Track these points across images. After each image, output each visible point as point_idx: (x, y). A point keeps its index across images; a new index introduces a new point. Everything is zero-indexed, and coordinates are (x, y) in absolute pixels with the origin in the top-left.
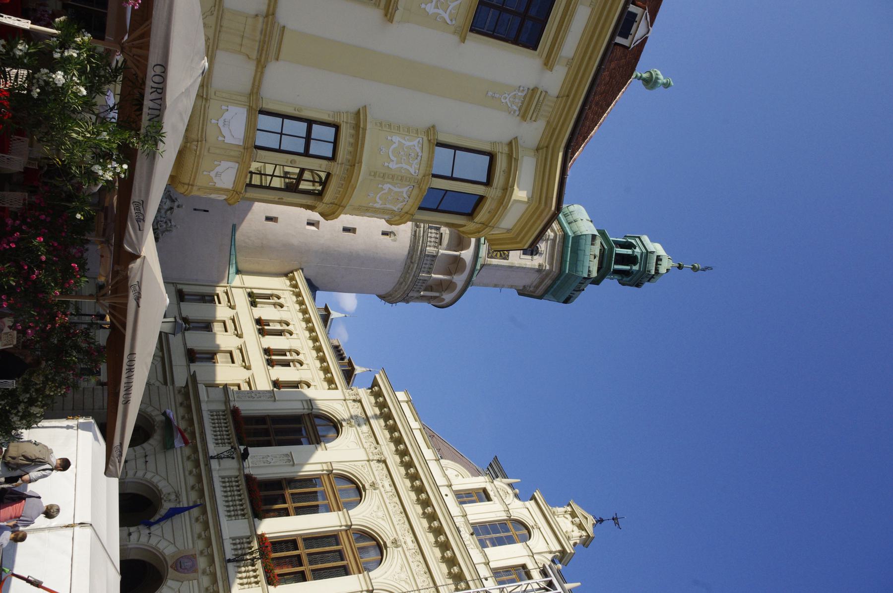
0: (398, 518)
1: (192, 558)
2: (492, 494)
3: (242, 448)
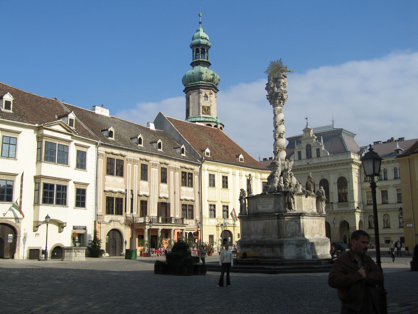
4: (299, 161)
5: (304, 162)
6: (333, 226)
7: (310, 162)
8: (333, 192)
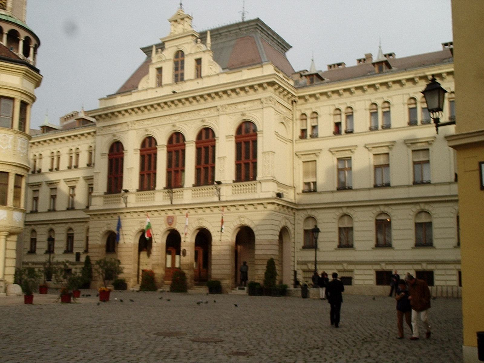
0: (163, 121)
1: (169, 218)
2: (159, 66)
3: (123, 192)
4: (157, 90)
5: (166, 91)
6: (219, 238)
7: (179, 90)
8: (224, 158)
